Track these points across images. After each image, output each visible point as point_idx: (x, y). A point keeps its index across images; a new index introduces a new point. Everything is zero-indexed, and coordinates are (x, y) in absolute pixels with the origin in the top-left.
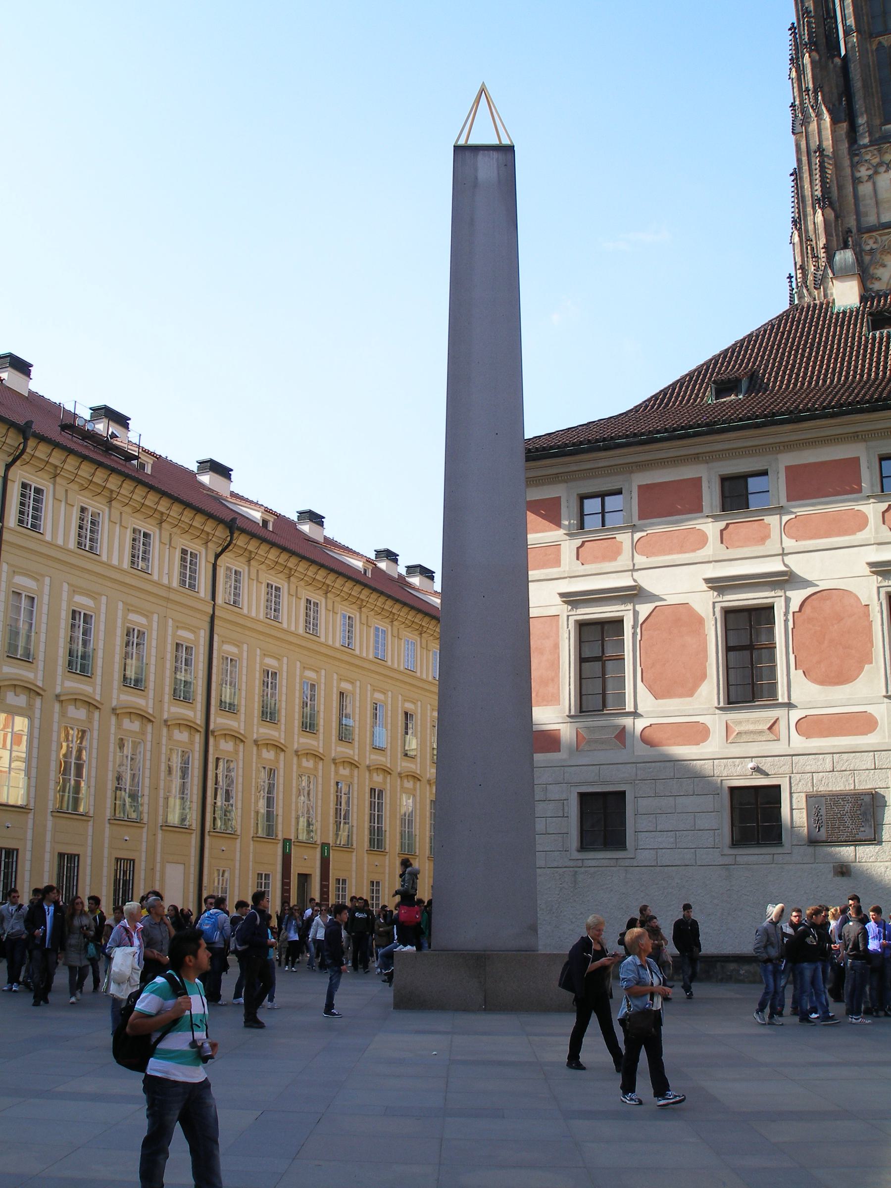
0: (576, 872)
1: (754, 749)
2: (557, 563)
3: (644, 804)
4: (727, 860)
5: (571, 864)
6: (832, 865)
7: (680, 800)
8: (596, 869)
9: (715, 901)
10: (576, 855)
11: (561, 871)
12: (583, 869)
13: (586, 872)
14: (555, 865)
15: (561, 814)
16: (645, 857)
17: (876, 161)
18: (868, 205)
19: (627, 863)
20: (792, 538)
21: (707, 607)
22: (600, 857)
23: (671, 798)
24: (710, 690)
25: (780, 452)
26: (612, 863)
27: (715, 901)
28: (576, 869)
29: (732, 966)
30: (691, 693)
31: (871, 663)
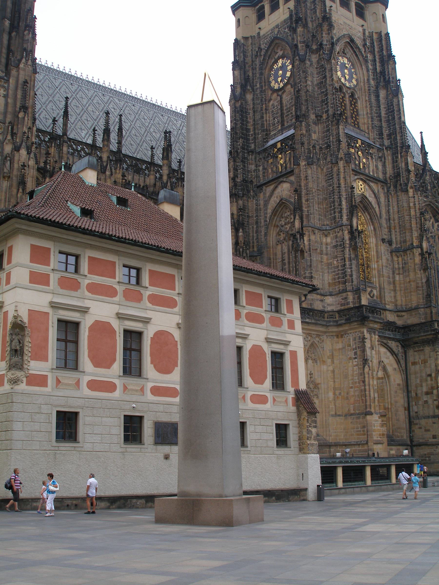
0: (56, 453)
1: (135, 398)
2: (48, 284)
3: (88, 419)
4: (121, 450)
5: (53, 448)
6: (163, 454)
7: (104, 419)
8: (66, 452)
9: (119, 470)
10: (55, 444)
11: (48, 452)
12: (58, 452)
13: (60, 453)
14: (45, 448)
15: (48, 421)
16: (88, 446)
19: (79, 449)
20: (150, 303)
21: (119, 327)
22: (66, 446)
23: (100, 418)
24: (117, 366)
25: (147, 262)
26: (73, 449)
27: (119, 470)
28: (56, 452)
29: (134, 501)
30: (109, 367)
31: (177, 366)
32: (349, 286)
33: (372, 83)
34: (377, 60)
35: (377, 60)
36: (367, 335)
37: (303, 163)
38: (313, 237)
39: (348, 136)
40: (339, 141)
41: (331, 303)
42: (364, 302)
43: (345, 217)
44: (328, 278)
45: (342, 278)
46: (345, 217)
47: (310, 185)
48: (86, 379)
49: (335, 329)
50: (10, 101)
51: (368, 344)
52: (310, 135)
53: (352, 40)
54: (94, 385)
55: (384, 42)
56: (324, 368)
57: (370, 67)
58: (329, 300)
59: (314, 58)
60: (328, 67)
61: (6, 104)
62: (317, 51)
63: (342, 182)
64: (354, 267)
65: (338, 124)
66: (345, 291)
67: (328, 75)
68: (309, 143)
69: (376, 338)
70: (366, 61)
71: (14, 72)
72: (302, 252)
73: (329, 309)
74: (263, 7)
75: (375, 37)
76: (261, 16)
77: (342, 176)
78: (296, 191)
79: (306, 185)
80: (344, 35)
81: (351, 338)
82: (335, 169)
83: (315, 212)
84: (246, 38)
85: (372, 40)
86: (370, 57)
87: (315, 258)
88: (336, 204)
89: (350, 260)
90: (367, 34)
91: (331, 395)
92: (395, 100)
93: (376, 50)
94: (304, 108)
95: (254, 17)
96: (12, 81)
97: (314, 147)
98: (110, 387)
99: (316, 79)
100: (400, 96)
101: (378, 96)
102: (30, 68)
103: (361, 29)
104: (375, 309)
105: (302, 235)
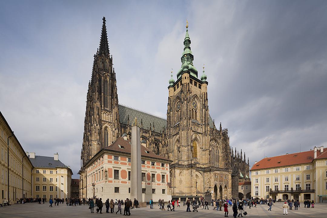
17: (104, 112)
18: (102, 117)
24: (127, 178)
30: (125, 179)
32: (190, 160)
33: (201, 107)
34: (203, 101)
35: (203, 101)
36: (193, 170)
37: (181, 130)
38: (182, 148)
39: (192, 122)
40: (190, 124)
41: (186, 163)
42: (193, 163)
43: (190, 143)
44: (186, 157)
45: (189, 157)
46: (190, 143)
47: (183, 136)
48: (121, 181)
49: (186, 169)
50: (113, 117)
51: (193, 172)
52: (183, 123)
53: (197, 96)
54: (122, 182)
55: (205, 95)
56: (184, 177)
57: (201, 103)
58: (185, 162)
59: (185, 102)
60: (188, 104)
61: (113, 118)
62: (186, 100)
63: (190, 134)
64: (191, 155)
65: (190, 120)
66: (189, 160)
67: (188, 107)
68: (183, 125)
69: (195, 170)
70: (200, 101)
71: (114, 110)
72: (180, 152)
73: (186, 164)
74: (175, 87)
75: (203, 94)
76: (175, 90)
77: (190, 133)
78: (179, 137)
79: (181, 136)
80: (194, 95)
81: (190, 170)
82: (188, 131)
83: (184, 142)
84: (171, 97)
85: (202, 95)
86: (201, 100)
87: (183, 153)
88: (188, 140)
89: (190, 153)
90: (201, 93)
91: (185, 183)
92: (207, 112)
93: (203, 98)
94: (182, 116)
95: (173, 90)
96: (113, 112)
97: (184, 126)
98: (126, 182)
99: (185, 108)
100: (208, 110)
101: (203, 111)
102: (117, 109)
103: (200, 92)
104: (195, 164)
105: (180, 148)
